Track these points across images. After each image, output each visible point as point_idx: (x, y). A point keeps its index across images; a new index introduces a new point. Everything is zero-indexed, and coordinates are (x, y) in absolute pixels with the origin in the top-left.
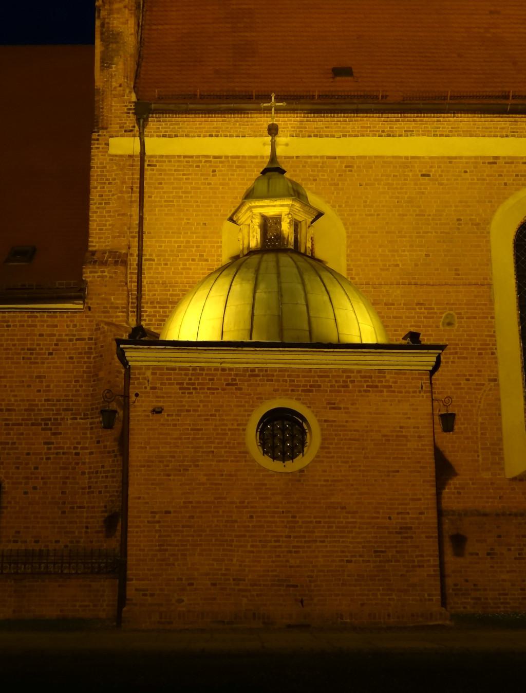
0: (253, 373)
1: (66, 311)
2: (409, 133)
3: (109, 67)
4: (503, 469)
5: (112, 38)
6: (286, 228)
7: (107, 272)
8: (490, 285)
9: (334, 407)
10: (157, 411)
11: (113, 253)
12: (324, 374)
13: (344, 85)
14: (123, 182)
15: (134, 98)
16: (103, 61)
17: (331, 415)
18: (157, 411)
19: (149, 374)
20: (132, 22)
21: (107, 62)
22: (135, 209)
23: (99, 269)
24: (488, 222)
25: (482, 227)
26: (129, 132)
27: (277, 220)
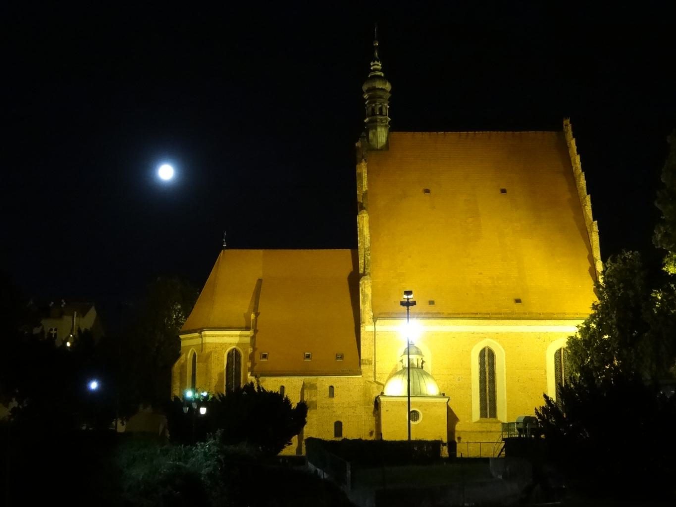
1: (356, 378)
3: (365, 304)
4: (472, 420)
5: (365, 295)
7: (367, 367)
8: (471, 369)
9: (425, 410)
10: (387, 411)
11: (368, 360)
12: (424, 403)
14: (370, 339)
15: (372, 314)
16: (363, 302)
17: (424, 412)
18: (387, 411)
19: (385, 403)
20: (371, 290)
21: (364, 302)
22: (373, 347)
23: (365, 366)
24: (471, 351)
25: (469, 353)
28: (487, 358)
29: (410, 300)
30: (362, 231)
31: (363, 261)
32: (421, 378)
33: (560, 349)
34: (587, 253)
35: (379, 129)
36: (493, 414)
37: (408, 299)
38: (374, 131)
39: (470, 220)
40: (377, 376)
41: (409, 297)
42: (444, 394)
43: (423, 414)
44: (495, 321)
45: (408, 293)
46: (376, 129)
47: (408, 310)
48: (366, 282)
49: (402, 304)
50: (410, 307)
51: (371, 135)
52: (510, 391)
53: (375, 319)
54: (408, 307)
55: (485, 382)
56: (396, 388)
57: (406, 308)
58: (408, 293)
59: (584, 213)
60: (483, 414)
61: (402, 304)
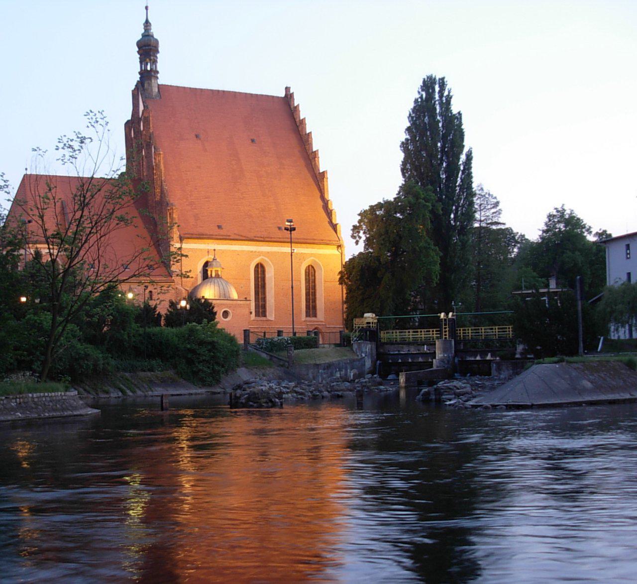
0: (222, 304)
2: (235, 245)
6: (219, 273)
9: (234, 310)
13: (221, 232)
24: (250, 265)
26: (178, 242)
27: (218, 271)
28: (260, 270)
29: (292, 226)
30: (158, 165)
31: (159, 190)
32: (229, 288)
33: (309, 266)
34: (319, 194)
35: (153, 81)
36: (264, 314)
37: (290, 225)
38: (149, 82)
39: (234, 162)
40: (183, 283)
41: (292, 224)
42: (246, 298)
43: (233, 313)
44: (212, 241)
45: (290, 221)
46: (151, 81)
47: (291, 234)
48: (174, 208)
49: (286, 229)
50: (293, 232)
51: (146, 85)
52: (277, 295)
53: (181, 239)
54: (291, 231)
55: (258, 287)
56: (208, 293)
57: (289, 232)
58: (290, 221)
59: (313, 163)
60: (257, 314)
61: (286, 229)
